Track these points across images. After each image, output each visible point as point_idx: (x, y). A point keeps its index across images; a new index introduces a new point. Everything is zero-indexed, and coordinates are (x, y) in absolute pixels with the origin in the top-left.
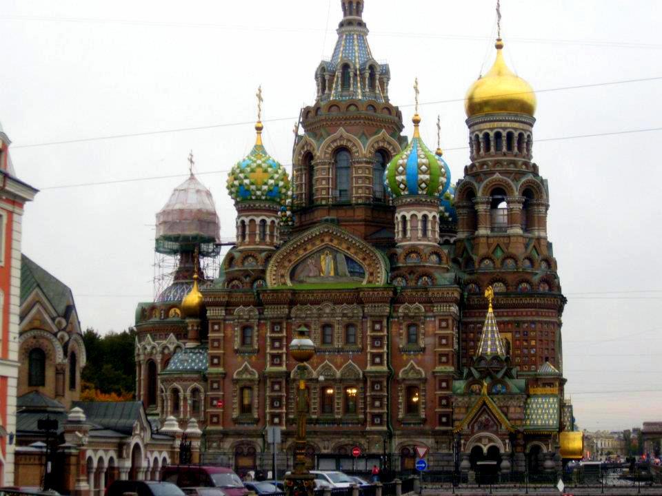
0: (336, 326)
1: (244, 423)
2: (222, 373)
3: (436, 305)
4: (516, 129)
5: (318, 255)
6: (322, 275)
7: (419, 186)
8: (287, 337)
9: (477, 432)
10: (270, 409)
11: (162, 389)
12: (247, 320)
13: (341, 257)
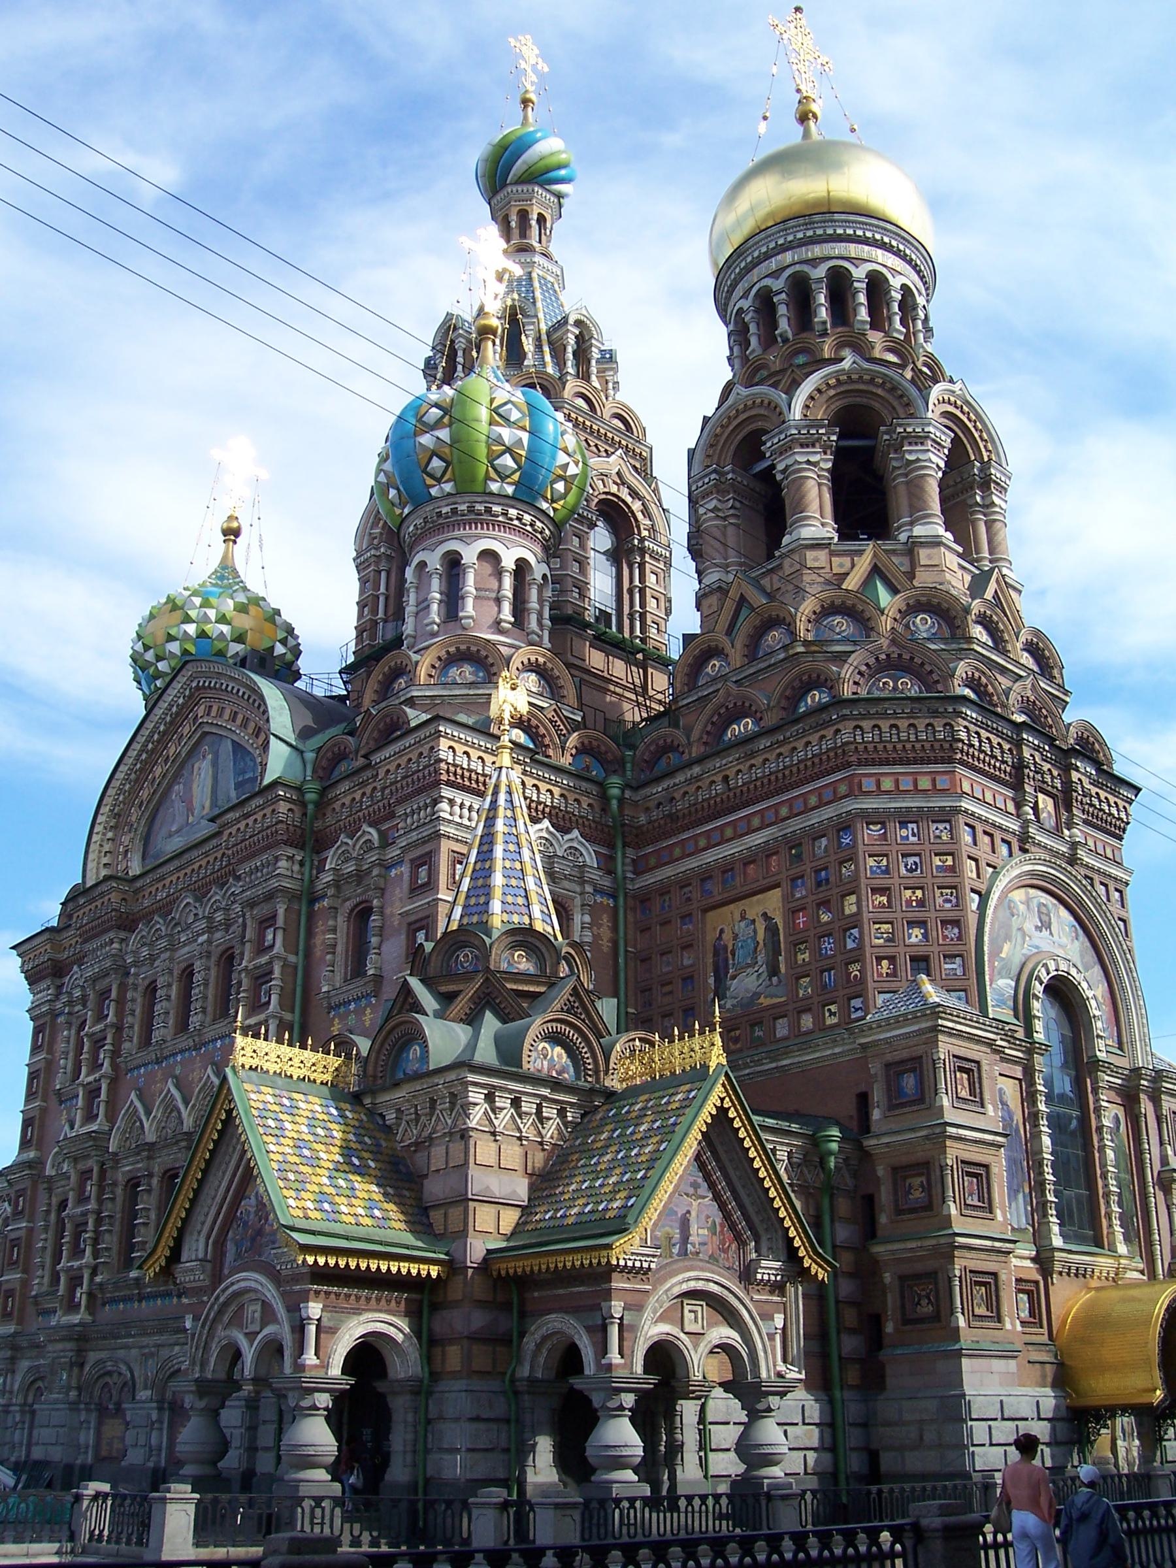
0: (198, 966)
3: (400, 811)
4: (814, 262)
5: (188, 766)
7: (425, 471)
8: (119, 1028)
9: (231, 1275)
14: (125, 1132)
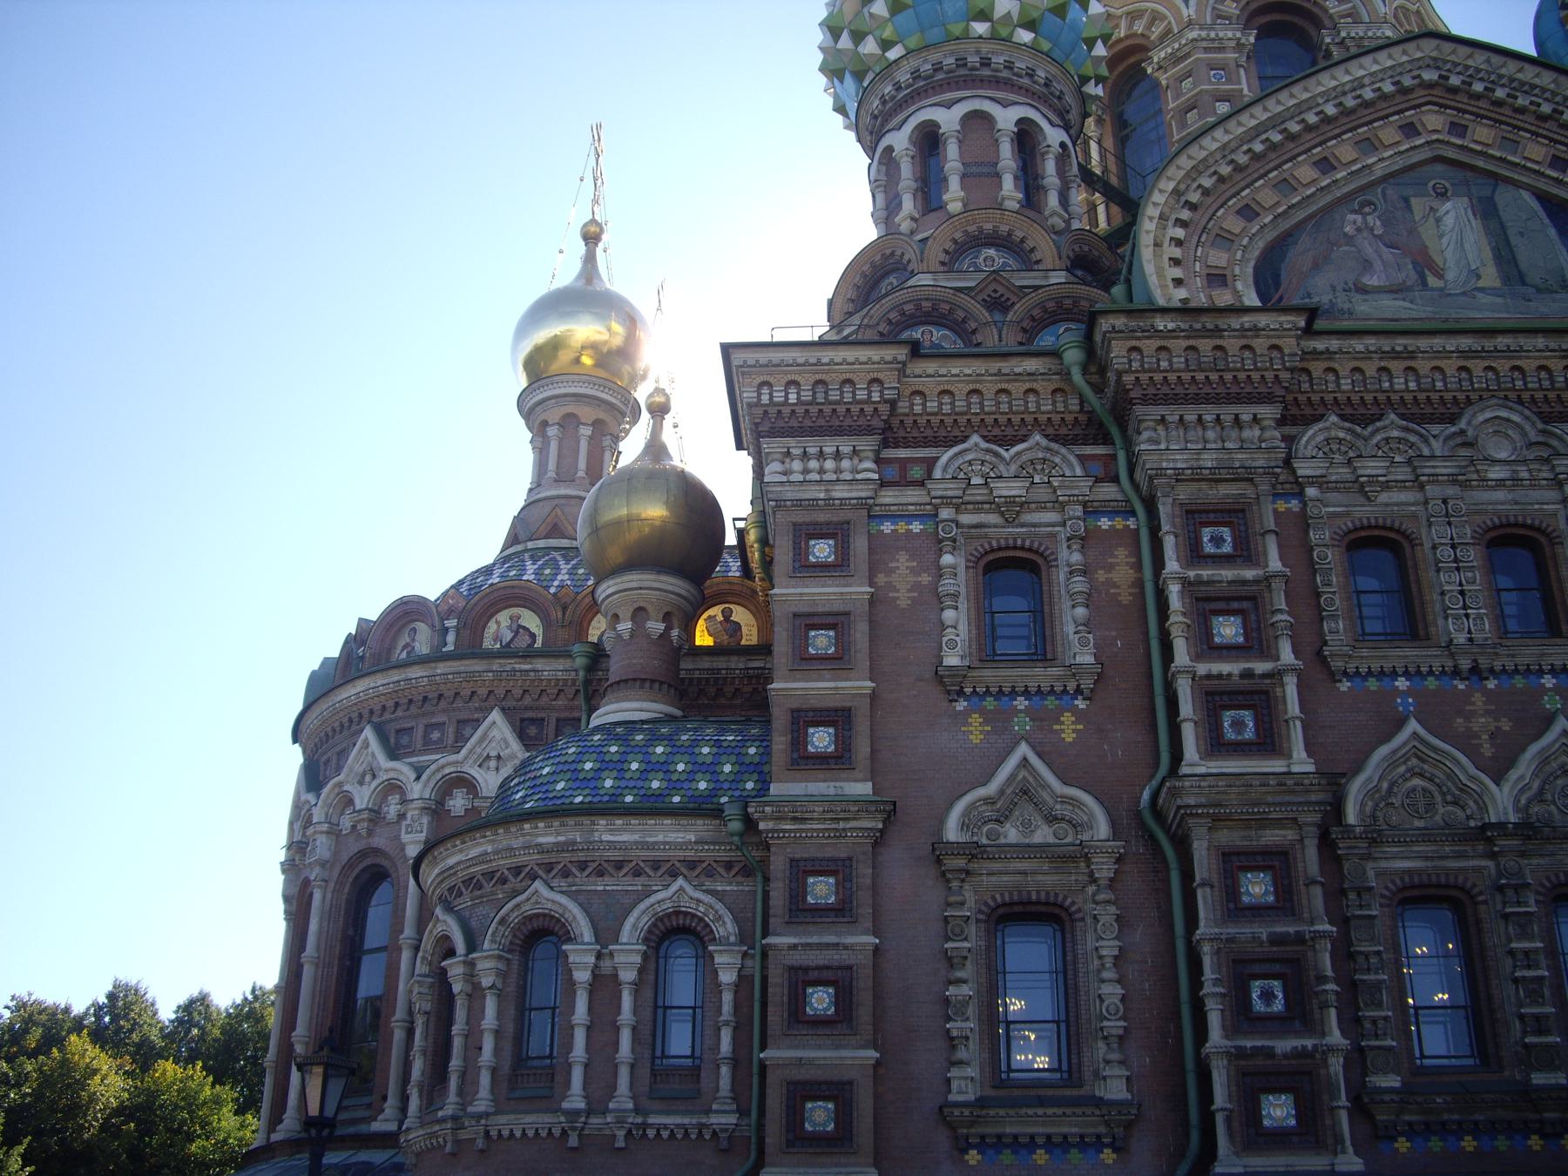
1: (1032, 1144)
2: (863, 805)
6: (1432, 281)
10: (1231, 1030)
11: (446, 938)
12: (1011, 509)
13: (1519, 207)
14: (1377, 789)
